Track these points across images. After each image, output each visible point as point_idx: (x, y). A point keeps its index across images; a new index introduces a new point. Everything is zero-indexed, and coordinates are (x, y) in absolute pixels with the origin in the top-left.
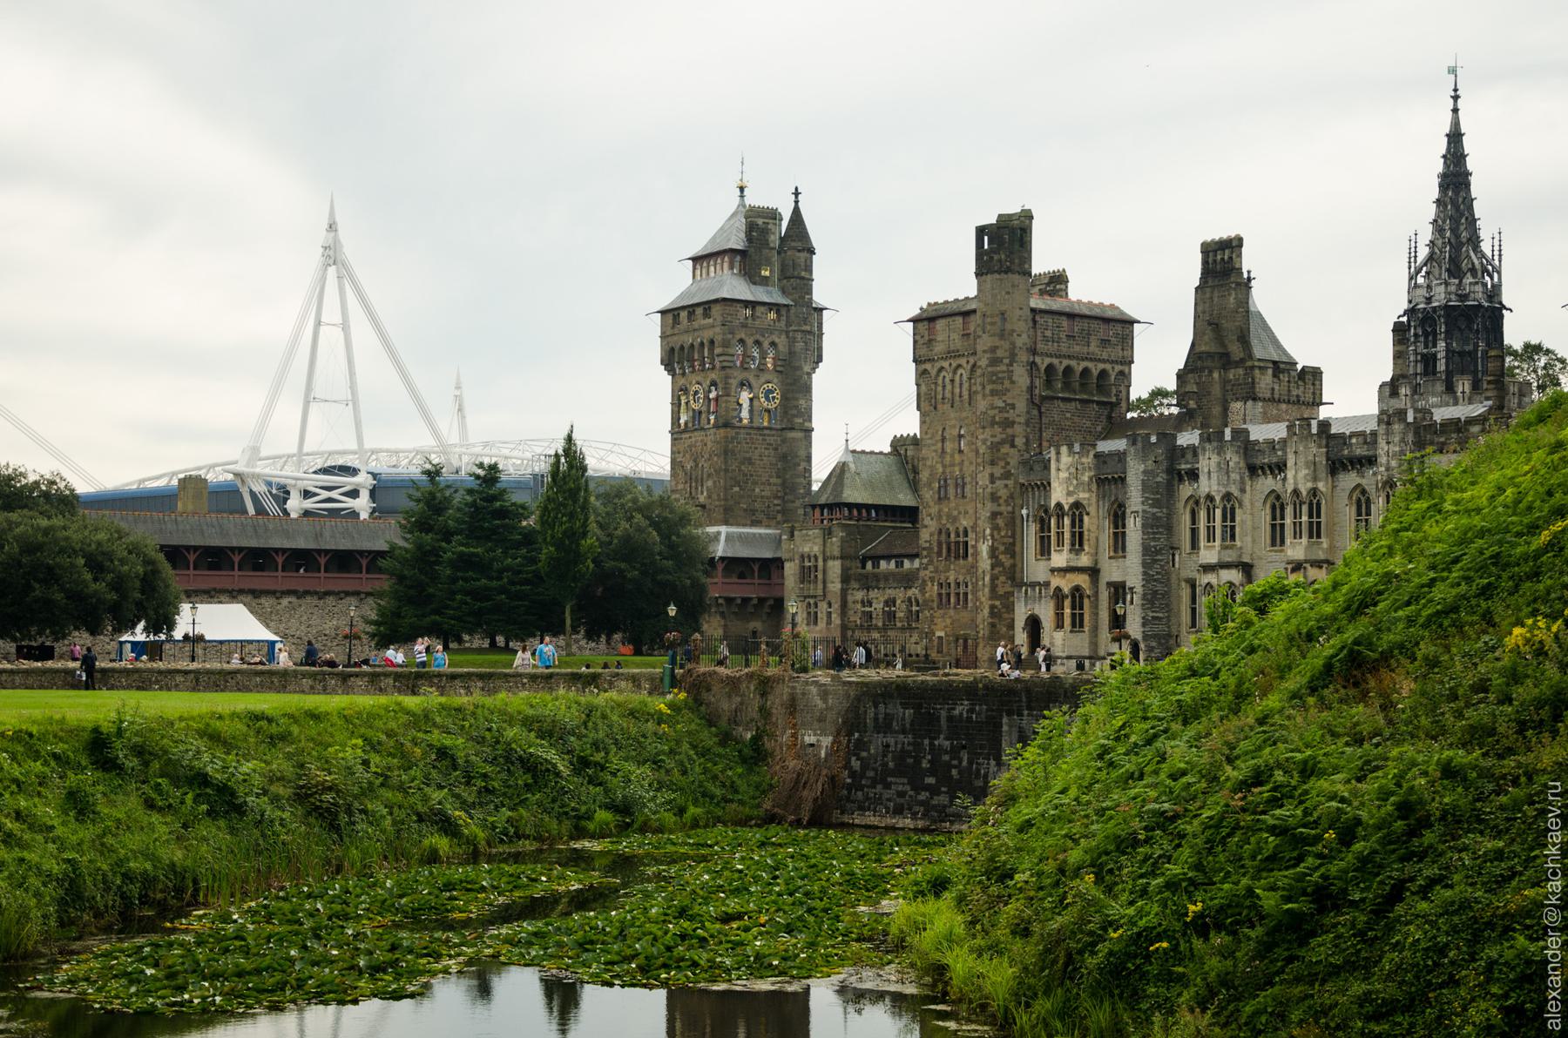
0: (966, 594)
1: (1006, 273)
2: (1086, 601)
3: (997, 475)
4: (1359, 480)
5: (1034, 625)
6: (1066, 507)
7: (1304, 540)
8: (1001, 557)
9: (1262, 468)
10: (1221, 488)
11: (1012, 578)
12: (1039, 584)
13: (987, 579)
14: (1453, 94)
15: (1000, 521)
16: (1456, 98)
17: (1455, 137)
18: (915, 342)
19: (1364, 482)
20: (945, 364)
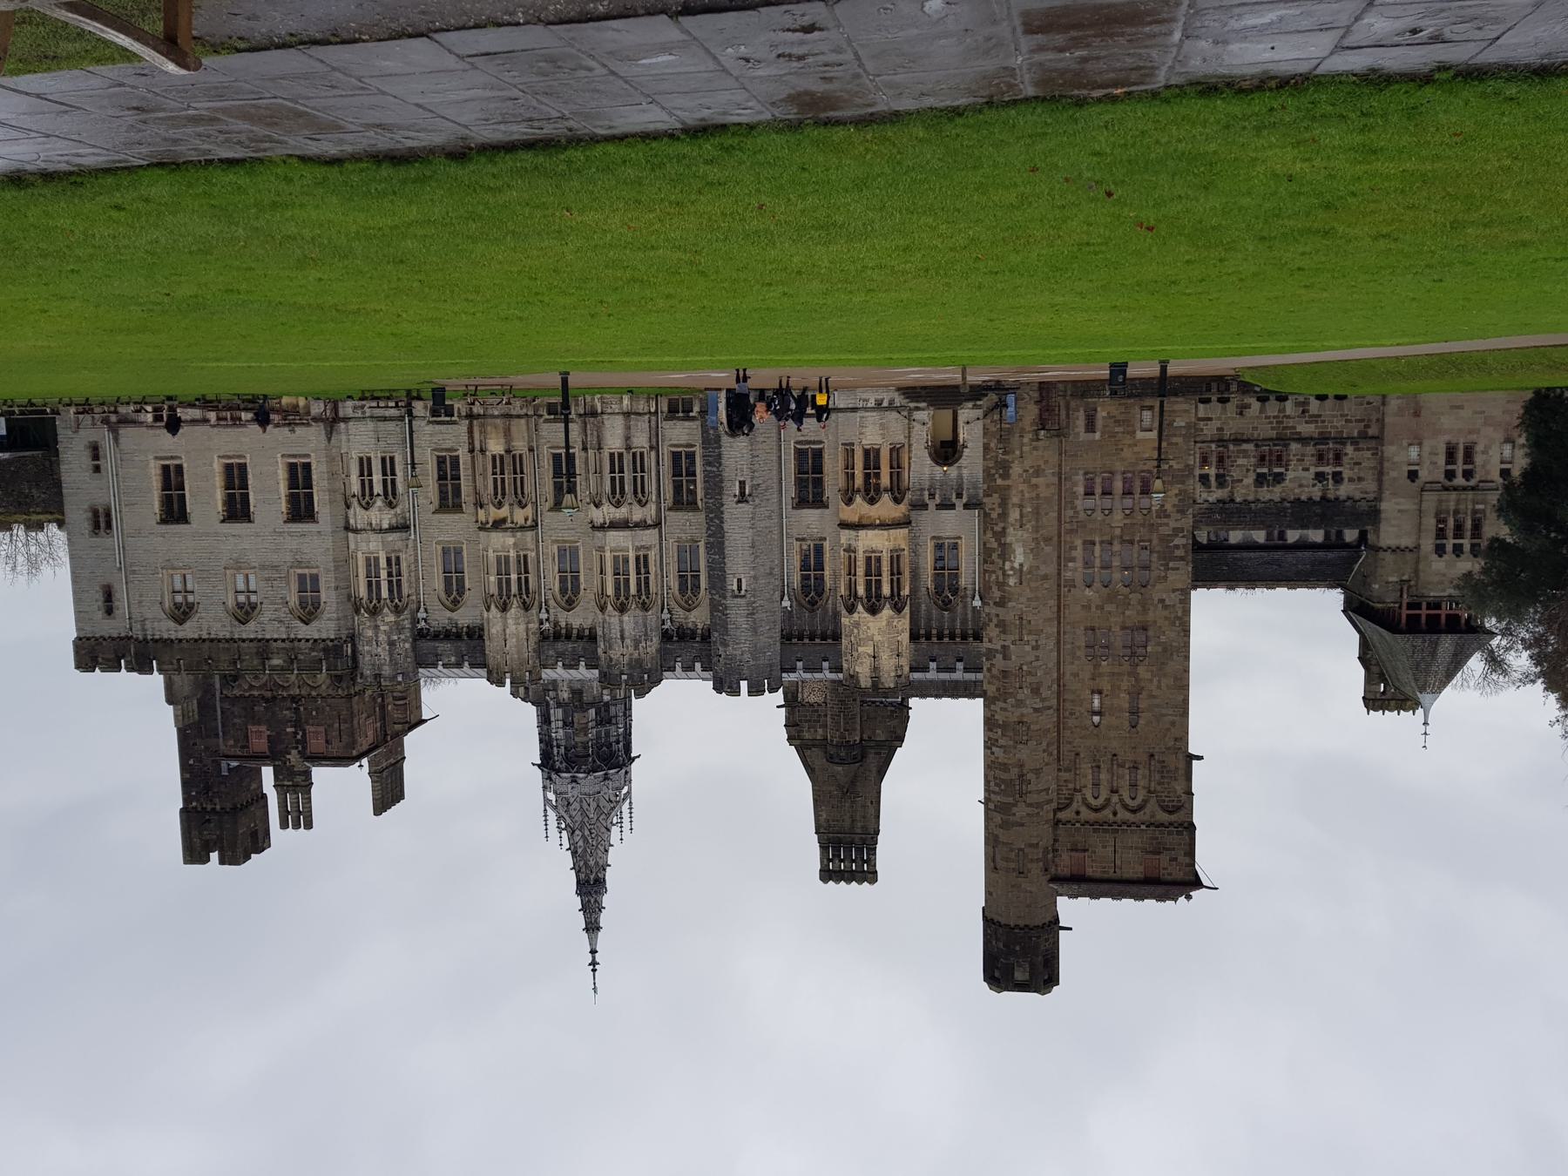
0: (1089, 493)
1: (992, 920)
2: (842, 483)
3: (999, 656)
4: (454, 615)
5: (947, 451)
6: (860, 608)
7: (491, 554)
8: (995, 545)
9: (580, 637)
10: (607, 618)
11: (986, 515)
12: (941, 507)
13: (1014, 515)
14: (597, 967)
15: (997, 594)
16: (594, 963)
17: (592, 927)
18: (1191, 852)
19: (448, 614)
20: (1123, 815)
